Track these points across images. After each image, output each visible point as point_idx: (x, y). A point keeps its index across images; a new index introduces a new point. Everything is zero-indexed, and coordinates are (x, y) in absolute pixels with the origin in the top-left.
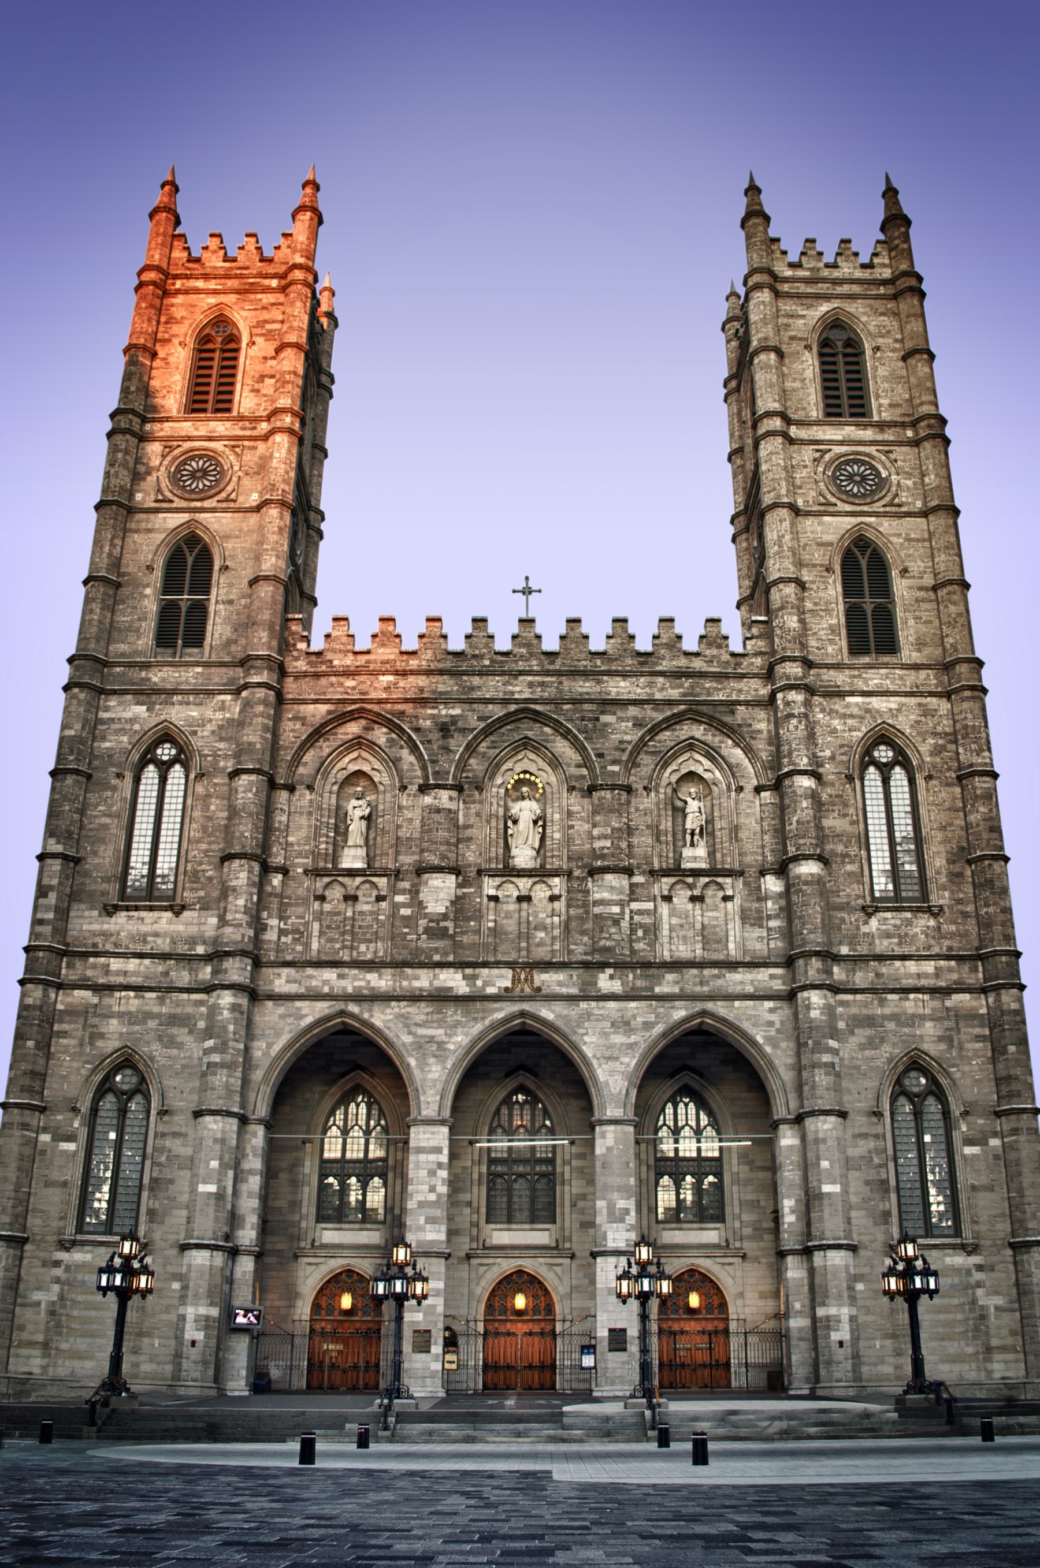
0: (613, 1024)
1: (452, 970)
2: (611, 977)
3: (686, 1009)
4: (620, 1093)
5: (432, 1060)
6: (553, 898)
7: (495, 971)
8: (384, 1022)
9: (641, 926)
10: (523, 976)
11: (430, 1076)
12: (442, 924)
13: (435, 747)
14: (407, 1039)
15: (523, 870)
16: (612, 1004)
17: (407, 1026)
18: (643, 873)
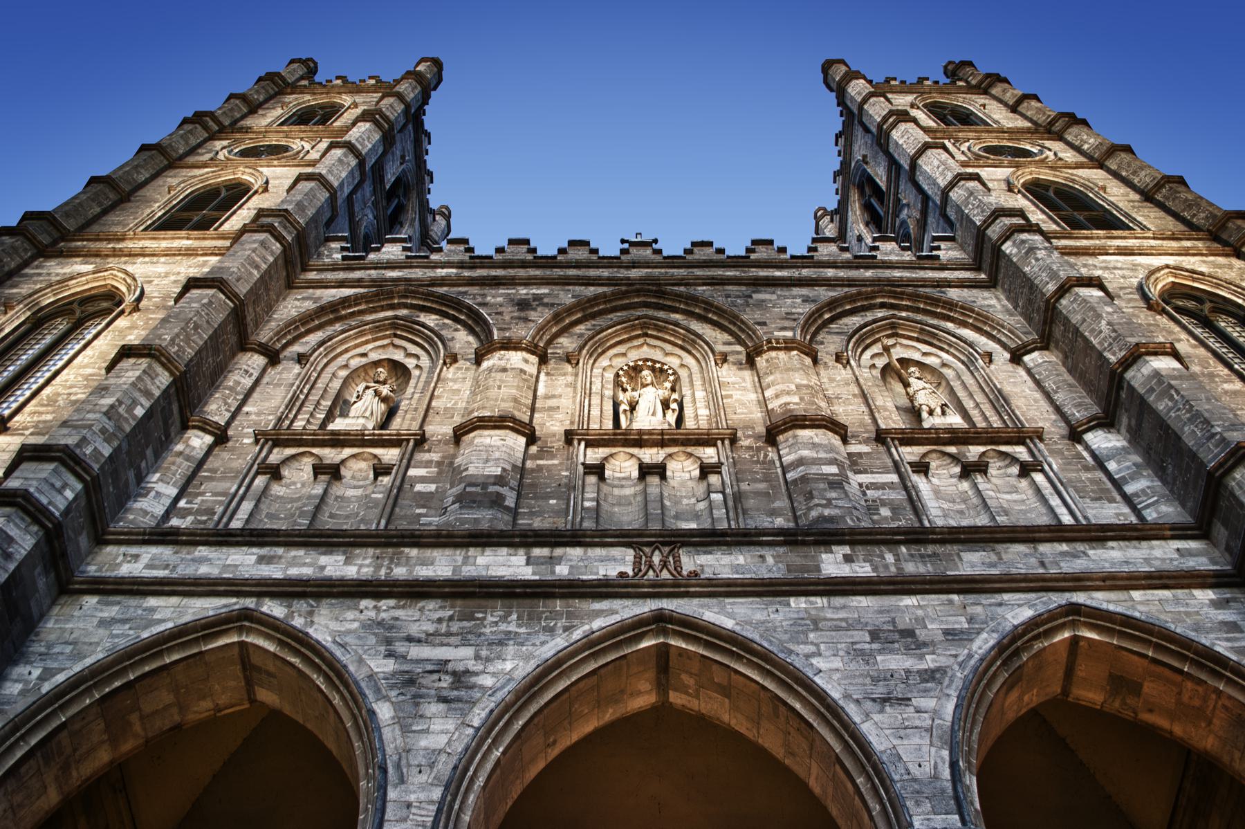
0: (875, 635)
1: (504, 550)
2: (848, 559)
3: (1032, 606)
4: (936, 777)
5: (434, 708)
6: (706, 470)
7: (599, 551)
8: (334, 634)
9: (884, 503)
10: (656, 559)
11: (424, 742)
12: (491, 489)
13: (507, 318)
14: (383, 666)
15: (650, 432)
16: (863, 602)
17: (389, 642)
18: (866, 441)
